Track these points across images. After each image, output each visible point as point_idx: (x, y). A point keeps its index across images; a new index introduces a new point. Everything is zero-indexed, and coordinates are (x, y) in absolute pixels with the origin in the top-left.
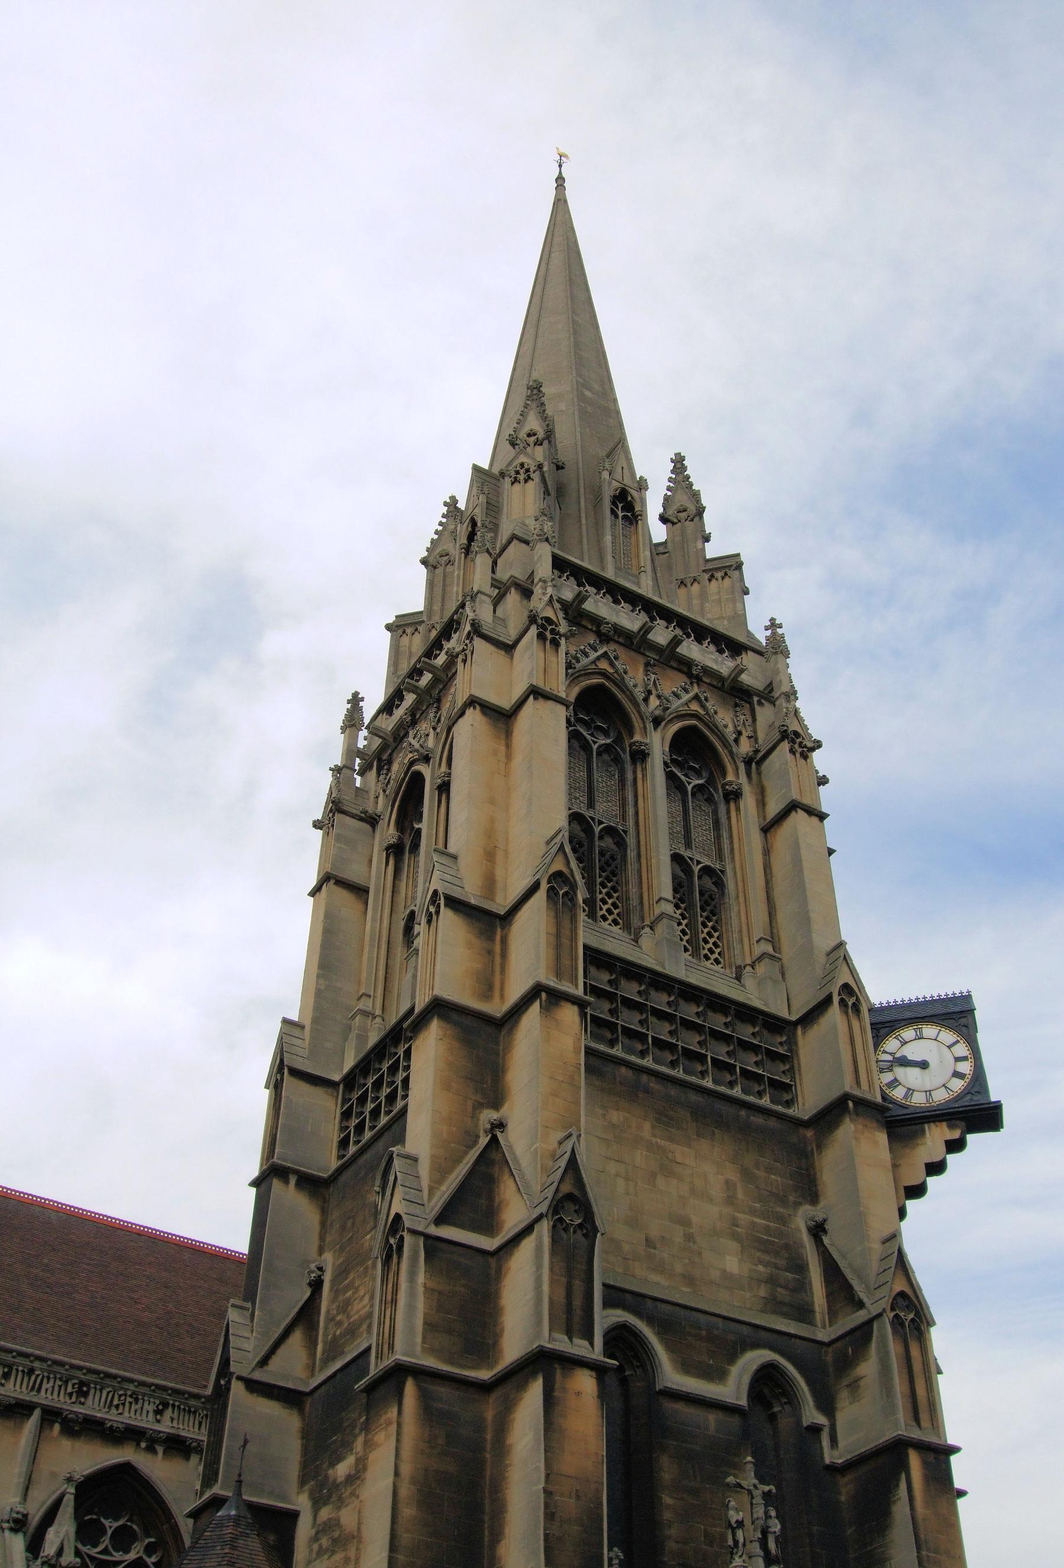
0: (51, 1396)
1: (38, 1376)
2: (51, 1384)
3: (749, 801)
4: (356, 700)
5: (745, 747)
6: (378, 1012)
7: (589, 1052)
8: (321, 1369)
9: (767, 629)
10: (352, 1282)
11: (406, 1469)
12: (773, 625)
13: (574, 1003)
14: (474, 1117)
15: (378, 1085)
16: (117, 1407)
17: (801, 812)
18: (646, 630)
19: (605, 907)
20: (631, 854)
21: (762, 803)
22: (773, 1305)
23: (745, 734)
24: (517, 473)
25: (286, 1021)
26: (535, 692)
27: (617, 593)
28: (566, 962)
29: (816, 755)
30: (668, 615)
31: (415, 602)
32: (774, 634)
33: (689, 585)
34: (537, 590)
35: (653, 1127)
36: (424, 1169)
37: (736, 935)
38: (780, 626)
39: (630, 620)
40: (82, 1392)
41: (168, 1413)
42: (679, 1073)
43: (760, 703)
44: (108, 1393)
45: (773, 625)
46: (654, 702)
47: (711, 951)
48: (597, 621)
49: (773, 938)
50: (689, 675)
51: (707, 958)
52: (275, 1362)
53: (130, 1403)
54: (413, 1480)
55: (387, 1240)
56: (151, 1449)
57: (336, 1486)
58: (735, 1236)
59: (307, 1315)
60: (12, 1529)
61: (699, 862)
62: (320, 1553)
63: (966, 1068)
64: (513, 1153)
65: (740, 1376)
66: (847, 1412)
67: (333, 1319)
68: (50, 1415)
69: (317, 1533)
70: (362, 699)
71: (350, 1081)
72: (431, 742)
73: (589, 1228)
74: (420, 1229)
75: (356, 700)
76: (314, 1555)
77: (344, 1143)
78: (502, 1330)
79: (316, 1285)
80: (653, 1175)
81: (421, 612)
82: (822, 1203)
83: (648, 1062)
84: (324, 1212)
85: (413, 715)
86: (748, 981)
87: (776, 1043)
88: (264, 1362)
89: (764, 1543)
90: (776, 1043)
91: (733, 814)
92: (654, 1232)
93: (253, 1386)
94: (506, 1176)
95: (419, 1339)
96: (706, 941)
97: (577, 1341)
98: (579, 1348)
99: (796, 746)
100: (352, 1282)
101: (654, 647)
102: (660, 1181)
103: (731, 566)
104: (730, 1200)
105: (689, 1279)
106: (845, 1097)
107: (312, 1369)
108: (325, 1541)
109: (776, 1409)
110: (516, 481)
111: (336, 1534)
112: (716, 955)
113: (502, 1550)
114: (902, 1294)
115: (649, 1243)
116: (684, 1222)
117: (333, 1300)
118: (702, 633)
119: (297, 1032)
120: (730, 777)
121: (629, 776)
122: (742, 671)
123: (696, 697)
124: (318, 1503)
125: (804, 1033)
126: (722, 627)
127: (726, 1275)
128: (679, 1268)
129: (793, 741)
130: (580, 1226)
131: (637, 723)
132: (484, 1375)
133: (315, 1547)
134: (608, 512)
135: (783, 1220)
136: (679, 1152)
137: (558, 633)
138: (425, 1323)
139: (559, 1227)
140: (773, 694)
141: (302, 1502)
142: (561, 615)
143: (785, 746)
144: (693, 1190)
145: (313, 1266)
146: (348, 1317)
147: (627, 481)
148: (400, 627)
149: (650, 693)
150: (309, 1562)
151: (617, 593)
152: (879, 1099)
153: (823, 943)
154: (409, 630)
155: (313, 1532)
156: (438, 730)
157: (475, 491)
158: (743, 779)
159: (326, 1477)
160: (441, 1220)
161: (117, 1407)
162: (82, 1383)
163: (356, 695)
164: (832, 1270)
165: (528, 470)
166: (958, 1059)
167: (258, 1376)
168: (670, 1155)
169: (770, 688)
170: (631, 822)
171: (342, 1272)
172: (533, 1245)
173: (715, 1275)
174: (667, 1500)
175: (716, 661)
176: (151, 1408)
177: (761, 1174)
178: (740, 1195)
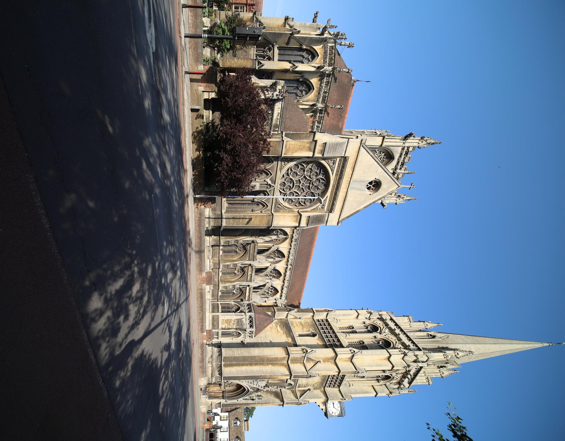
24: (446, 355)
71: (327, 320)
82: (313, 390)
106: (328, 399)
135: (311, 386)
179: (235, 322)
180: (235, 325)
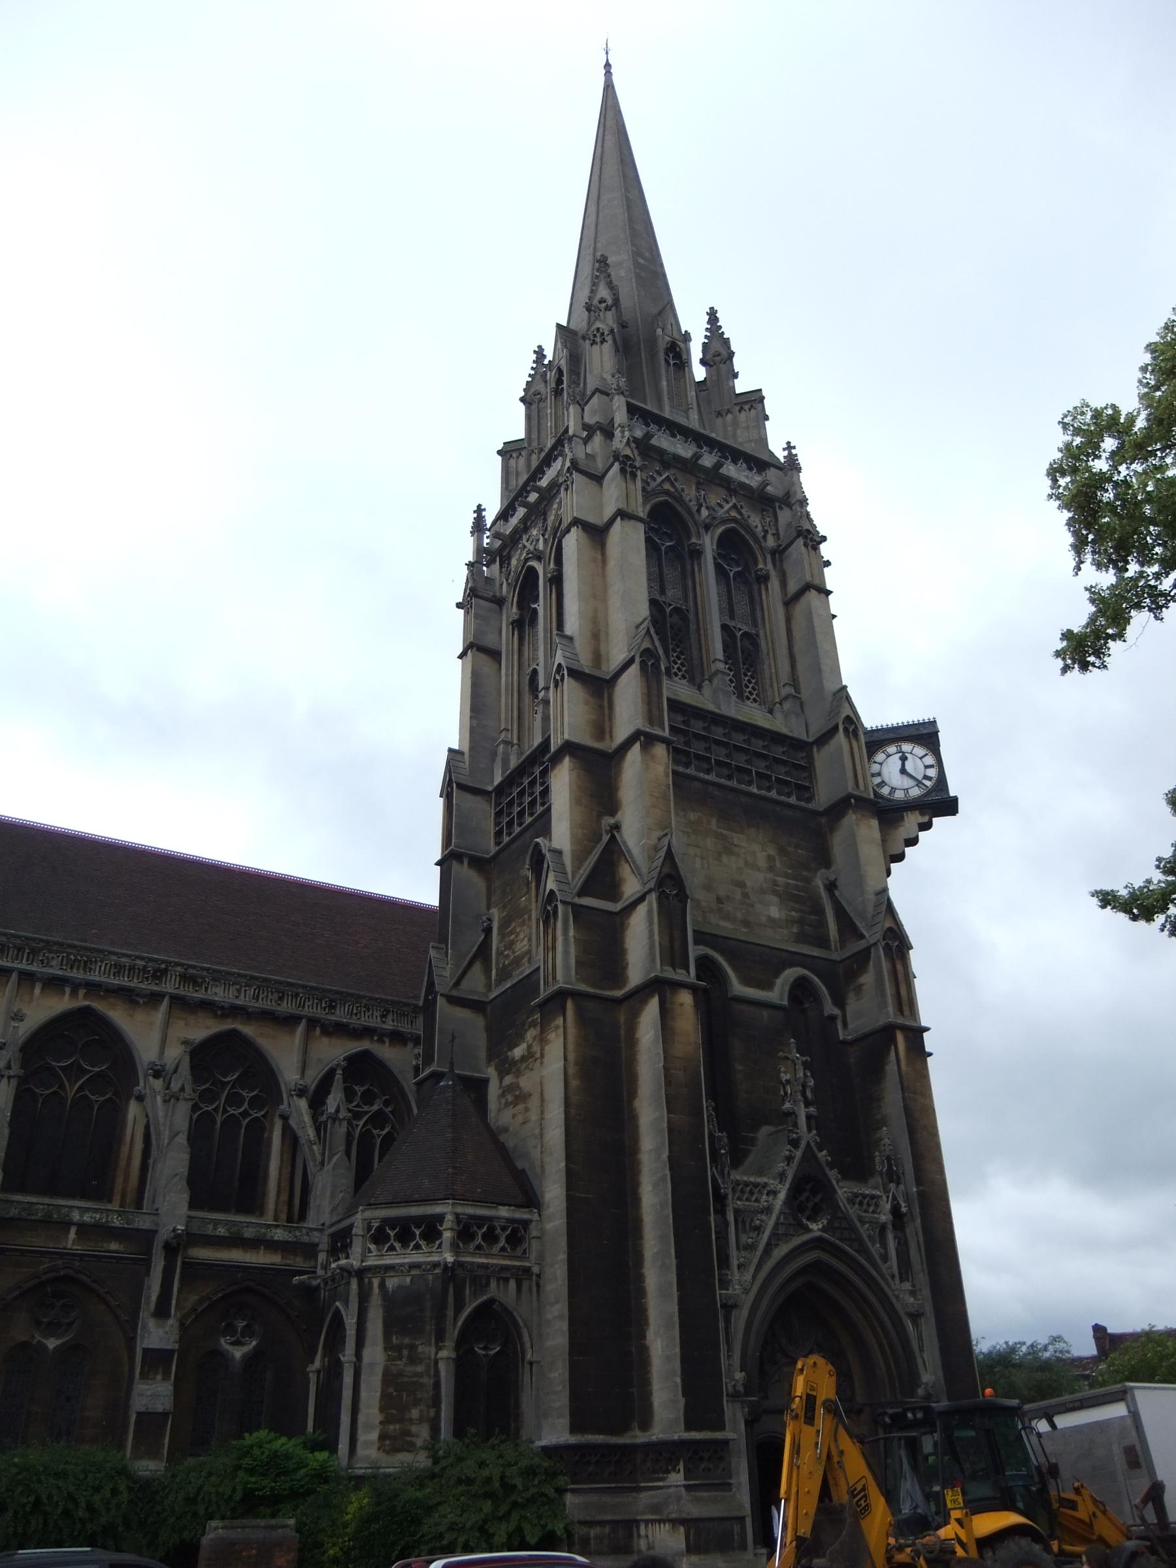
0: (312, 1009)
1: (302, 997)
2: (311, 1003)
3: (774, 583)
4: (479, 510)
5: (771, 542)
6: (515, 741)
7: (675, 773)
8: (496, 986)
9: (784, 449)
10: (514, 928)
11: (572, 1057)
12: (789, 447)
13: (663, 742)
14: (598, 822)
15: (521, 794)
16: (356, 1014)
17: (813, 592)
18: (697, 456)
19: (676, 666)
20: (693, 627)
21: (784, 584)
22: (801, 938)
23: (770, 532)
24: (595, 336)
25: (451, 750)
26: (622, 514)
27: (675, 429)
28: (655, 712)
29: (823, 547)
30: (712, 444)
31: (517, 431)
32: (790, 454)
33: (724, 415)
34: (617, 433)
35: (718, 821)
36: (567, 860)
37: (768, 681)
38: (794, 448)
39: (684, 450)
40: (331, 1007)
41: (390, 1017)
42: (733, 783)
43: (781, 508)
44: (349, 1005)
45: (789, 447)
46: (705, 513)
47: (751, 693)
48: (661, 452)
49: (795, 683)
50: (729, 490)
51: (748, 699)
52: (465, 984)
53: (365, 1012)
54: (576, 1063)
55: (545, 908)
56: (381, 1041)
57: (514, 1063)
58: (775, 893)
59: (483, 952)
60: (298, 1095)
61: (740, 630)
62: (507, 1104)
63: (932, 773)
64: (626, 846)
65: (783, 985)
66: (852, 1005)
67: (502, 953)
68: (313, 1023)
69: (504, 1092)
70: (484, 510)
71: (500, 790)
72: (541, 546)
73: (683, 896)
74: (569, 900)
75: (479, 510)
76: (503, 1106)
77: (499, 834)
78: (627, 964)
79: (488, 931)
80: (720, 854)
81: (523, 439)
82: (833, 868)
83: (712, 777)
84: (488, 880)
85: (525, 524)
86: (779, 715)
87: (800, 759)
88: (458, 983)
89: (804, 1094)
90: (800, 759)
91: (764, 592)
92: (722, 893)
93: (453, 1000)
94: (623, 862)
95: (573, 973)
96: (747, 687)
97: (679, 971)
98: (679, 975)
99: (808, 541)
100: (514, 928)
101: (703, 469)
102: (725, 859)
103: (755, 399)
104: (771, 869)
105: (746, 923)
106: (850, 796)
107: (489, 987)
108: (510, 1098)
109: (806, 1006)
110: (594, 343)
111: (517, 1093)
112: (754, 696)
113: (637, 1103)
114: (890, 929)
115: (719, 900)
116: (742, 885)
117: (501, 941)
118: (736, 455)
119: (458, 757)
120: (761, 566)
121: (689, 567)
122: (768, 484)
123: (735, 506)
124: (502, 1074)
125: (818, 750)
126: (748, 448)
127: (770, 919)
128: (739, 915)
129: (806, 538)
130: (676, 895)
131: (693, 529)
132: (618, 993)
133: (503, 1101)
134: (663, 362)
135: (808, 881)
136: (737, 838)
137: (635, 467)
138: (577, 961)
139: (662, 898)
140: (790, 499)
141: (491, 1072)
142: (636, 452)
143: (801, 541)
144: (746, 863)
145: (484, 918)
146: (514, 952)
147: (676, 335)
148: (508, 452)
149: (701, 505)
150: (499, 1110)
151: (675, 429)
152: (872, 796)
153: (830, 687)
154: (514, 455)
155: (501, 1091)
156: (546, 537)
157: (559, 345)
158: (770, 566)
159: (507, 1057)
160: (580, 894)
161: (356, 1014)
162: (331, 1001)
163: (479, 506)
164: (842, 914)
165: (603, 334)
166: (927, 767)
167: (454, 993)
168: (730, 840)
169: (788, 495)
170: (691, 603)
171: (504, 924)
172: (646, 908)
173: (764, 919)
174: (739, 1067)
175: (747, 477)
176: (378, 1014)
177: (791, 849)
178: (778, 864)
179: (399, 1348)
180: (420, 1349)
